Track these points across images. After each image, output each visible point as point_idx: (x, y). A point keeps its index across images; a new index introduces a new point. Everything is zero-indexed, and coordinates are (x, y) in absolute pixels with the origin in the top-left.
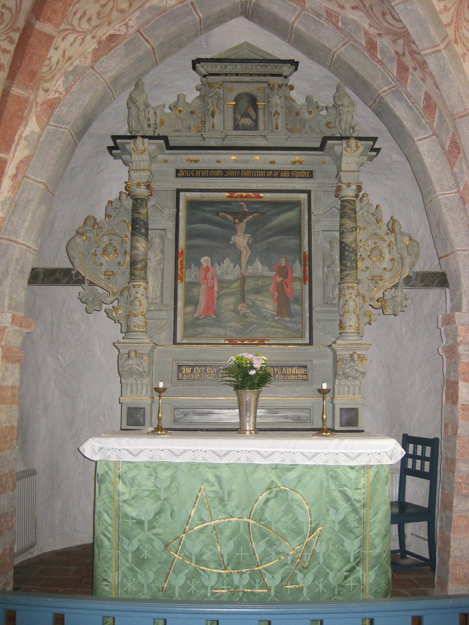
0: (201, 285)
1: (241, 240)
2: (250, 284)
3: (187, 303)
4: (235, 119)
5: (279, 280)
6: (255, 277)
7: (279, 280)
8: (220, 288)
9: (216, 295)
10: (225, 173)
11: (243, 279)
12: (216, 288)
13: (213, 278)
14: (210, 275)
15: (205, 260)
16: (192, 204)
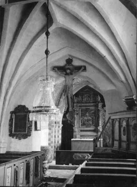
1: (87, 114)
3: (81, 122)
6: (90, 119)
10: (86, 106)
11: (88, 119)
15: (83, 117)
16: (81, 110)
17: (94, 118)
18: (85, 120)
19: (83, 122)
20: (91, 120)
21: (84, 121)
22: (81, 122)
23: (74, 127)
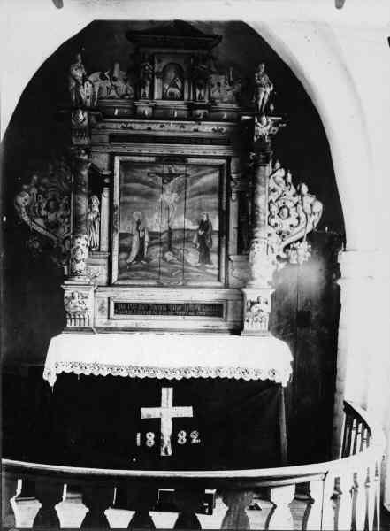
0: (132, 235)
2: (176, 236)
4: (163, 89)
5: (201, 233)
7: (201, 233)
8: (151, 239)
9: (146, 244)
10: (156, 140)
11: (170, 232)
12: (147, 239)
13: (143, 230)
14: (141, 228)
17: (216, 227)
18: (153, 235)
19: (134, 254)
20: (195, 240)
21: (142, 240)
22: (123, 249)
23: (67, 278)
